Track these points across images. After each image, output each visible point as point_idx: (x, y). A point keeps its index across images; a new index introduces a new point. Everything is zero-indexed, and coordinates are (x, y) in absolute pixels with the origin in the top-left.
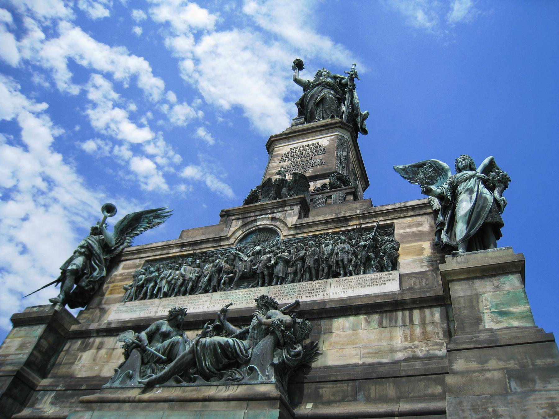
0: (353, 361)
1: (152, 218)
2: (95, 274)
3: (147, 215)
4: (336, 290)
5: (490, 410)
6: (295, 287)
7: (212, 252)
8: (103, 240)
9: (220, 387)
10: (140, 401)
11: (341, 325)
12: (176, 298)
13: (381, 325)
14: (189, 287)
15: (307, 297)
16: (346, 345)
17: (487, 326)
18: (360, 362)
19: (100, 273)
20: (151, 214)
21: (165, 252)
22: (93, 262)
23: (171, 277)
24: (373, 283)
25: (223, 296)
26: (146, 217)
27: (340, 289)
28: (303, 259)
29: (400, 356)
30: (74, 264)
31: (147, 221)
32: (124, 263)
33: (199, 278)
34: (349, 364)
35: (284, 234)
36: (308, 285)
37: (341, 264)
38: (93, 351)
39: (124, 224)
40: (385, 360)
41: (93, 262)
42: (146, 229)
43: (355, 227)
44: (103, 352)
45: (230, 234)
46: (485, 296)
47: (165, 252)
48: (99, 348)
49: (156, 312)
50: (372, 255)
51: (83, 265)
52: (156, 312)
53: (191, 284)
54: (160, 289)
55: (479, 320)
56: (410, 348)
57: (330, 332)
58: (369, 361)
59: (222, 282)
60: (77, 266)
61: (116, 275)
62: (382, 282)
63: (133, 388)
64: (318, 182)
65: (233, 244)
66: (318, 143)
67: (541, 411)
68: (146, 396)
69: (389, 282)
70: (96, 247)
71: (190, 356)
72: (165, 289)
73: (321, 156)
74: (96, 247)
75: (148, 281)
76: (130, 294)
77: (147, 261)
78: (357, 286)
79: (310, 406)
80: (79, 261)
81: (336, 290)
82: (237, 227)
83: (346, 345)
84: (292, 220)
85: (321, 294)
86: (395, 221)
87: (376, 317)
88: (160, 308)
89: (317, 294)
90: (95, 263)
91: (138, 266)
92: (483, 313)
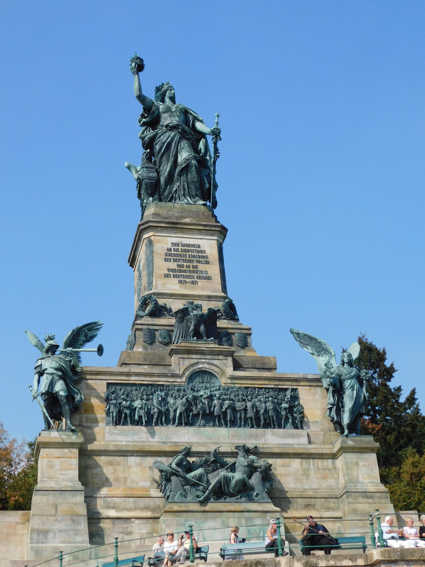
1: (87, 331)
6: (245, 432)
15: (255, 440)
20: (87, 328)
24: (293, 436)
25: (196, 430)
27: (274, 438)
28: (245, 410)
37: (271, 419)
39: (70, 339)
43: (273, 386)
54: (140, 417)
62: (298, 436)
65: (184, 382)
69: (302, 437)
71: (218, 485)
85: (263, 439)
89: (261, 439)
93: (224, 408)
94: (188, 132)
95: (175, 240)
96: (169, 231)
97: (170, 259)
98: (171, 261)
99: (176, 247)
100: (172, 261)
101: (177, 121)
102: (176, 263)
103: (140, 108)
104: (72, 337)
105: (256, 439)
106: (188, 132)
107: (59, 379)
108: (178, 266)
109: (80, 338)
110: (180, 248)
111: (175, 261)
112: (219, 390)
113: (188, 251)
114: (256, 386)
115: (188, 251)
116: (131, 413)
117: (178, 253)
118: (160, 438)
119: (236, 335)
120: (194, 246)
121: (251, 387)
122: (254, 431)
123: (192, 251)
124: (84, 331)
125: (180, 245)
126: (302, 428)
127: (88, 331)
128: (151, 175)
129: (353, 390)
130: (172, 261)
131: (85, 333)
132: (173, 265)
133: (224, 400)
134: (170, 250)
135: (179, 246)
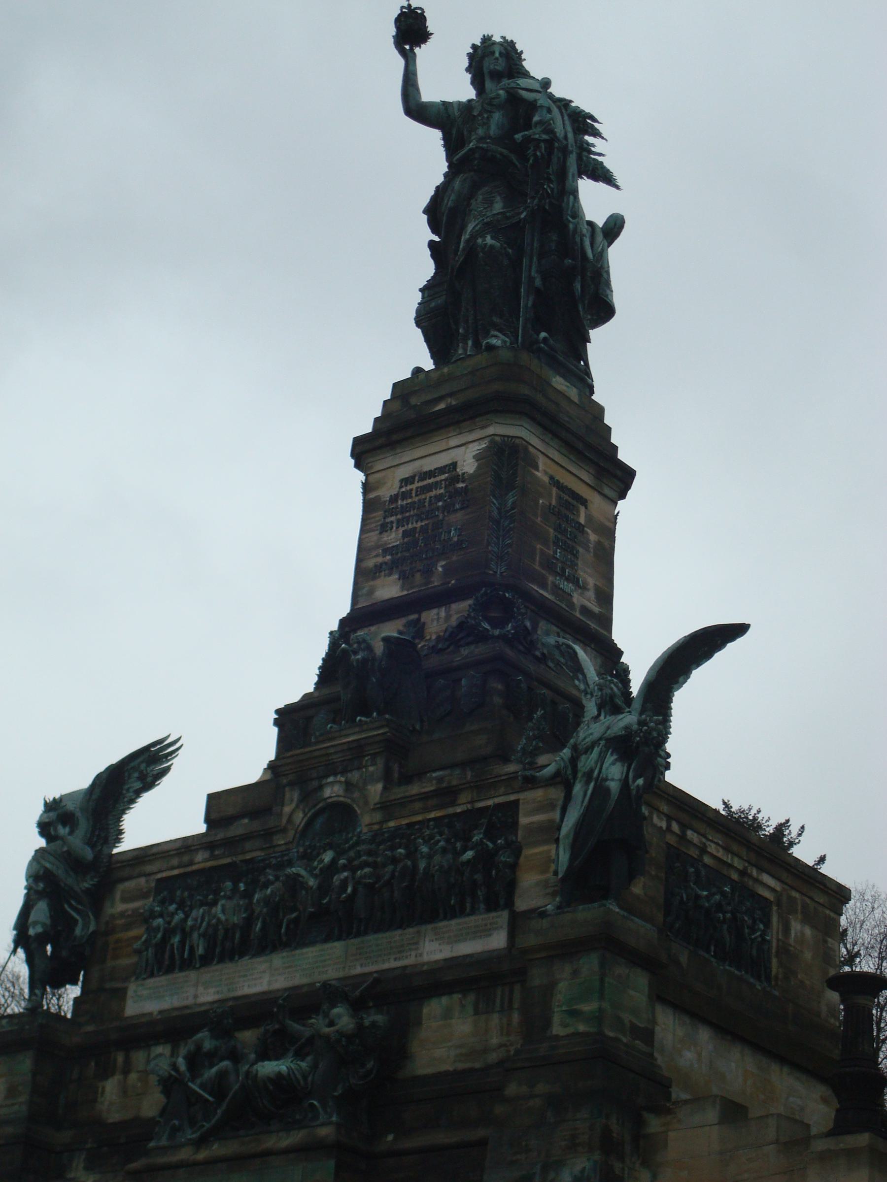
0: (443, 1068)
1: (143, 766)
2: (78, 931)
3: (132, 764)
4: (434, 948)
5: (524, 1143)
7: (263, 860)
8: (68, 852)
9: (280, 1134)
10: (196, 1164)
11: (433, 1008)
12: (220, 966)
13: (477, 1012)
14: (237, 940)
15: (395, 959)
16: (447, 1036)
17: (554, 1032)
18: (451, 1069)
19: (86, 926)
21: (186, 859)
22: (66, 906)
23: (204, 924)
26: (132, 768)
27: (435, 945)
29: (493, 1057)
30: (35, 923)
31: (136, 775)
32: (121, 887)
33: (249, 922)
34: (439, 1073)
35: (367, 820)
36: (397, 938)
38: (118, 1077)
39: (94, 797)
40: (477, 1065)
41: (66, 906)
42: (138, 793)
44: (133, 1076)
45: (284, 821)
46: (561, 985)
47: (186, 859)
48: (126, 1072)
49: (196, 996)
50: (478, 877)
51: (51, 917)
52: (196, 996)
53: (237, 936)
54: (192, 949)
55: (548, 1023)
56: (505, 1045)
57: (419, 1022)
58: (461, 1066)
59: (283, 930)
60: (44, 925)
61: (113, 917)
63: (183, 1145)
64: (454, 606)
65: (291, 842)
66: (454, 465)
67: (563, 1143)
68: (202, 1155)
70: (60, 871)
72: (201, 951)
73: (459, 515)
74: (60, 871)
75: (169, 932)
76: (147, 960)
77: (159, 881)
78: (459, 938)
79: (390, 1138)
80: (41, 910)
81: (434, 948)
82: (294, 805)
83: (447, 1036)
84: (376, 790)
85: (413, 953)
86: (521, 796)
87: (471, 998)
88: (201, 989)
90: (71, 906)
91: (144, 895)
92: (554, 1012)
93: (349, 890)
94: (498, 156)
95: (405, 472)
96: (398, 451)
97: (392, 522)
98: (392, 528)
99: (409, 488)
100: (394, 525)
101: (481, 139)
102: (401, 530)
103: (436, 135)
104: (97, 791)
105: (398, 956)
106: (498, 156)
107: (39, 899)
108: (405, 534)
109: (126, 787)
110: (414, 486)
111: (400, 523)
112: (357, 843)
113: (429, 488)
114: (432, 815)
115: (429, 488)
116: (183, 942)
117: (409, 501)
118: (218, 992)
119: (463, 682)
120: (441, 470)
121: (419, 822)
122: (397, 938)
123: (436, 485)
124: (134, 769)
125: (417, 478)
126: (509, 904)
127: (148, 766)
128: (433, 304)
129: (587, 783)
130: (394, 525)
131: (141, 772)
132: (393, 538)
133: (353, 870)
134: (394, 499)
135: (413, 483)
